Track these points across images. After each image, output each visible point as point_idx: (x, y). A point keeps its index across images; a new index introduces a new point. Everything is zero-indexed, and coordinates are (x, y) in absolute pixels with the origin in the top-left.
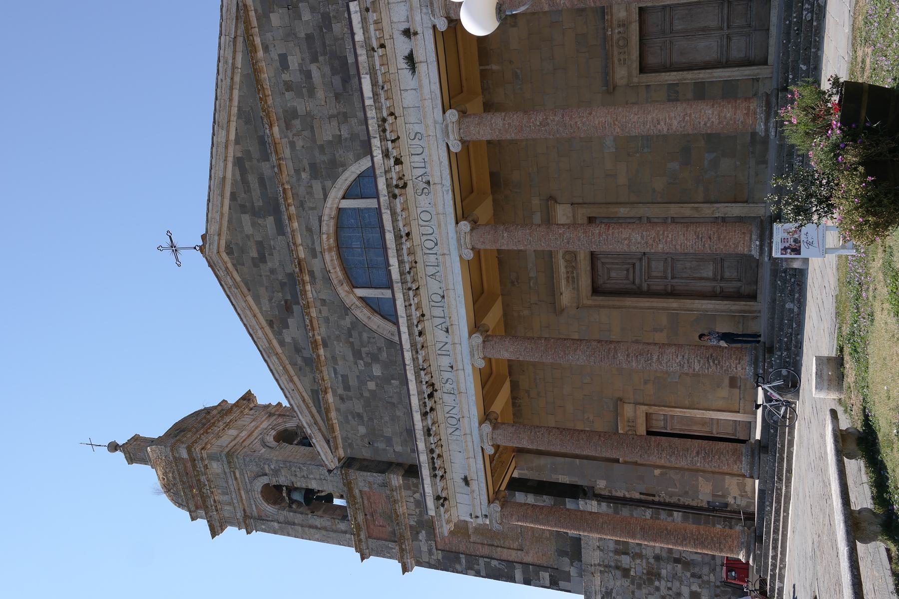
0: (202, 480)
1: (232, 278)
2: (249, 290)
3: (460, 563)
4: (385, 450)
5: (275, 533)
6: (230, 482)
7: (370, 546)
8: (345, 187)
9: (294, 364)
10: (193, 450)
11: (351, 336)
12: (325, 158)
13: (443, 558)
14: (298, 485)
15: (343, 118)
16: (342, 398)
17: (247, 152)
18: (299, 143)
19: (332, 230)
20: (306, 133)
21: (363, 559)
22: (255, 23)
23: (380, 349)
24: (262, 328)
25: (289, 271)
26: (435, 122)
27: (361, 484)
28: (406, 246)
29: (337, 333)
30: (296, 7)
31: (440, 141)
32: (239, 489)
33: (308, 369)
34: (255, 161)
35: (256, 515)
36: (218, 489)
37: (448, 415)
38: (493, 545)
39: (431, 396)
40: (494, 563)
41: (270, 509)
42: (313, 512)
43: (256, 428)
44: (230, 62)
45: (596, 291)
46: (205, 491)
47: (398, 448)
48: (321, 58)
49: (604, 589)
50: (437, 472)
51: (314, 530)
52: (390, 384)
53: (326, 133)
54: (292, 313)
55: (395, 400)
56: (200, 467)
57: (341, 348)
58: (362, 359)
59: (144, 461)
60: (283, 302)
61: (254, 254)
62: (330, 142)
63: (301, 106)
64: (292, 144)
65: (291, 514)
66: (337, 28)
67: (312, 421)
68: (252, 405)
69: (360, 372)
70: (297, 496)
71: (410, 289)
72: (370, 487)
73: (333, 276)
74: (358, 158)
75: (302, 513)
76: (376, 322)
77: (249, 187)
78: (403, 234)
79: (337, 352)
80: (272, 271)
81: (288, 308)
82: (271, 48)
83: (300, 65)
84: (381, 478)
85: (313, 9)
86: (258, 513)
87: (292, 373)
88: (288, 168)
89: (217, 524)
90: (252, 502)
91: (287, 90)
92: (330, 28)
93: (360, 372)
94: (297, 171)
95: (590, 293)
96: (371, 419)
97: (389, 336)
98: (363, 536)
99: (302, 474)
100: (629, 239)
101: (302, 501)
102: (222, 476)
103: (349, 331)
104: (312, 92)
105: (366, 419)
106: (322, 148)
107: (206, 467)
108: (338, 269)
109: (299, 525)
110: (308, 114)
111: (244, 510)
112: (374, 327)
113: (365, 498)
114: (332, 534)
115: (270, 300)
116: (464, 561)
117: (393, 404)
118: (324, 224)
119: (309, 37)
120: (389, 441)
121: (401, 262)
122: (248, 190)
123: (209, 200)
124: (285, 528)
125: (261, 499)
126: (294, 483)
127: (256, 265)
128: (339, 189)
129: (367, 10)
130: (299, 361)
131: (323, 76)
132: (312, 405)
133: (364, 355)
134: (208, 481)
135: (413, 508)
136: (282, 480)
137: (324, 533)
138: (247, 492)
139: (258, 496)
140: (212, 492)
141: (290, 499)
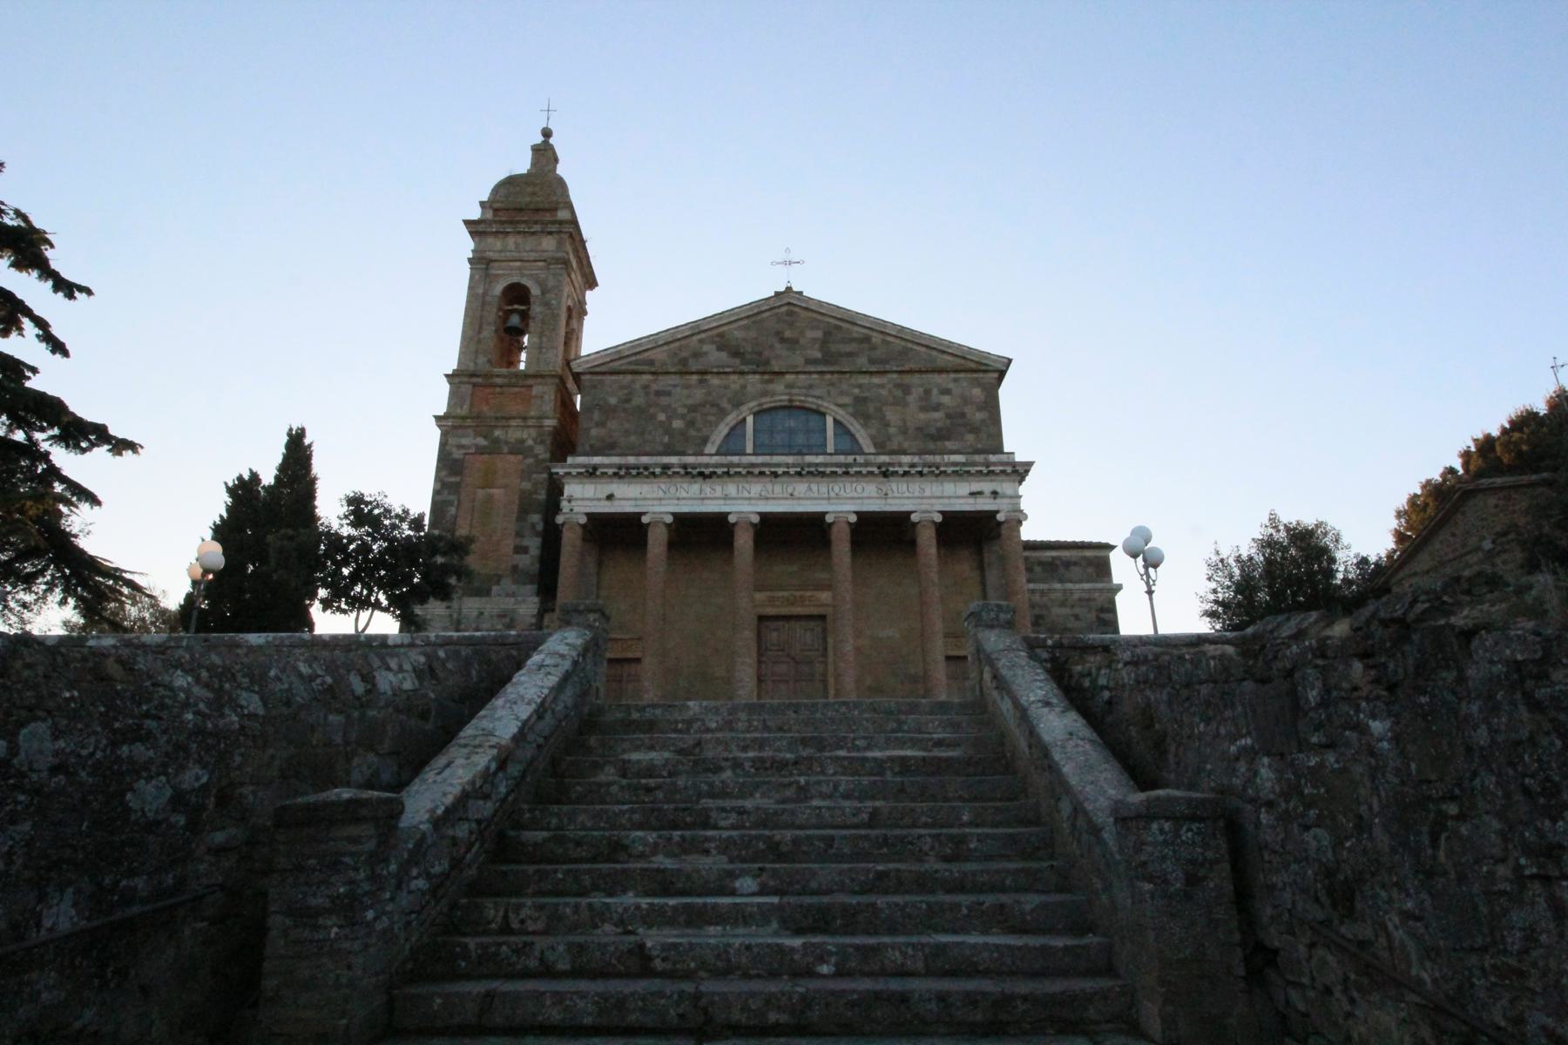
1: (766, 311)
5: (470, 288)
7: (462, 386)
8: (845, 422)
9: (680, 349)
11: (712, 405)
12: (871, 410)
13: (456, 460)
15: (904, 431)
19: (807, 405)
20: (891, 399)
21: (447, 376)
22: (975, 375)
23: (699, 430)
25: (773, 362)
26: (932, 505)
27: (540, 387)
28: (840, 471)
29: (714, 394)
38: (473, 511)
39: (701, 474)
40: (453, 510)
41: (498, 289)
45: (762, 618)
47: (594, 432)
48: (948, 422)
49: (429, 617)
53: (892, 415)
55: (648, 437)
57: (699, 394)
58: (689, 412)
60: (742, 351)
61: (788, 334)
62: (883, 418)
63: (911, 398)
64: (882, 386)
65: (495, 310)
66: (970, 438)
70: (515, 320)
71: (802, 469)
72: (535, 397)
73: (768, 399)
74: (873, 438)
76: (723, 429)
78: (850, 470)
80: (772, 347)
81: (736, 353)
85: (983, 421)
87: (672, 346)
89: (481, 228)
90: (509, 272)
92: (971, 431)
93: (675, 410)
94: (860, 386)
96: (625, 410)
97: (712, 438)
101: (509, 325)
103: (718, 405)
104: (924, 409)
105: (627, 406)
106: (879, 410)
107: (550, 233)
108: (773, 405)
110: (906, 405)
115: (745, 340)
116: (453, 479)
117: (642, 434)
118: (815, 400)
119: (963, 415)
120: (601, 424)
121: (826, 465)
127: (778, 333)
129: (1014, 467)
130: (684, 354)
131: (936, 420)
133: (693, 415)
136: (536, 309)
138: (519, 269)
139: (515, 280)
140: (519, 233)
141: (512, 311)
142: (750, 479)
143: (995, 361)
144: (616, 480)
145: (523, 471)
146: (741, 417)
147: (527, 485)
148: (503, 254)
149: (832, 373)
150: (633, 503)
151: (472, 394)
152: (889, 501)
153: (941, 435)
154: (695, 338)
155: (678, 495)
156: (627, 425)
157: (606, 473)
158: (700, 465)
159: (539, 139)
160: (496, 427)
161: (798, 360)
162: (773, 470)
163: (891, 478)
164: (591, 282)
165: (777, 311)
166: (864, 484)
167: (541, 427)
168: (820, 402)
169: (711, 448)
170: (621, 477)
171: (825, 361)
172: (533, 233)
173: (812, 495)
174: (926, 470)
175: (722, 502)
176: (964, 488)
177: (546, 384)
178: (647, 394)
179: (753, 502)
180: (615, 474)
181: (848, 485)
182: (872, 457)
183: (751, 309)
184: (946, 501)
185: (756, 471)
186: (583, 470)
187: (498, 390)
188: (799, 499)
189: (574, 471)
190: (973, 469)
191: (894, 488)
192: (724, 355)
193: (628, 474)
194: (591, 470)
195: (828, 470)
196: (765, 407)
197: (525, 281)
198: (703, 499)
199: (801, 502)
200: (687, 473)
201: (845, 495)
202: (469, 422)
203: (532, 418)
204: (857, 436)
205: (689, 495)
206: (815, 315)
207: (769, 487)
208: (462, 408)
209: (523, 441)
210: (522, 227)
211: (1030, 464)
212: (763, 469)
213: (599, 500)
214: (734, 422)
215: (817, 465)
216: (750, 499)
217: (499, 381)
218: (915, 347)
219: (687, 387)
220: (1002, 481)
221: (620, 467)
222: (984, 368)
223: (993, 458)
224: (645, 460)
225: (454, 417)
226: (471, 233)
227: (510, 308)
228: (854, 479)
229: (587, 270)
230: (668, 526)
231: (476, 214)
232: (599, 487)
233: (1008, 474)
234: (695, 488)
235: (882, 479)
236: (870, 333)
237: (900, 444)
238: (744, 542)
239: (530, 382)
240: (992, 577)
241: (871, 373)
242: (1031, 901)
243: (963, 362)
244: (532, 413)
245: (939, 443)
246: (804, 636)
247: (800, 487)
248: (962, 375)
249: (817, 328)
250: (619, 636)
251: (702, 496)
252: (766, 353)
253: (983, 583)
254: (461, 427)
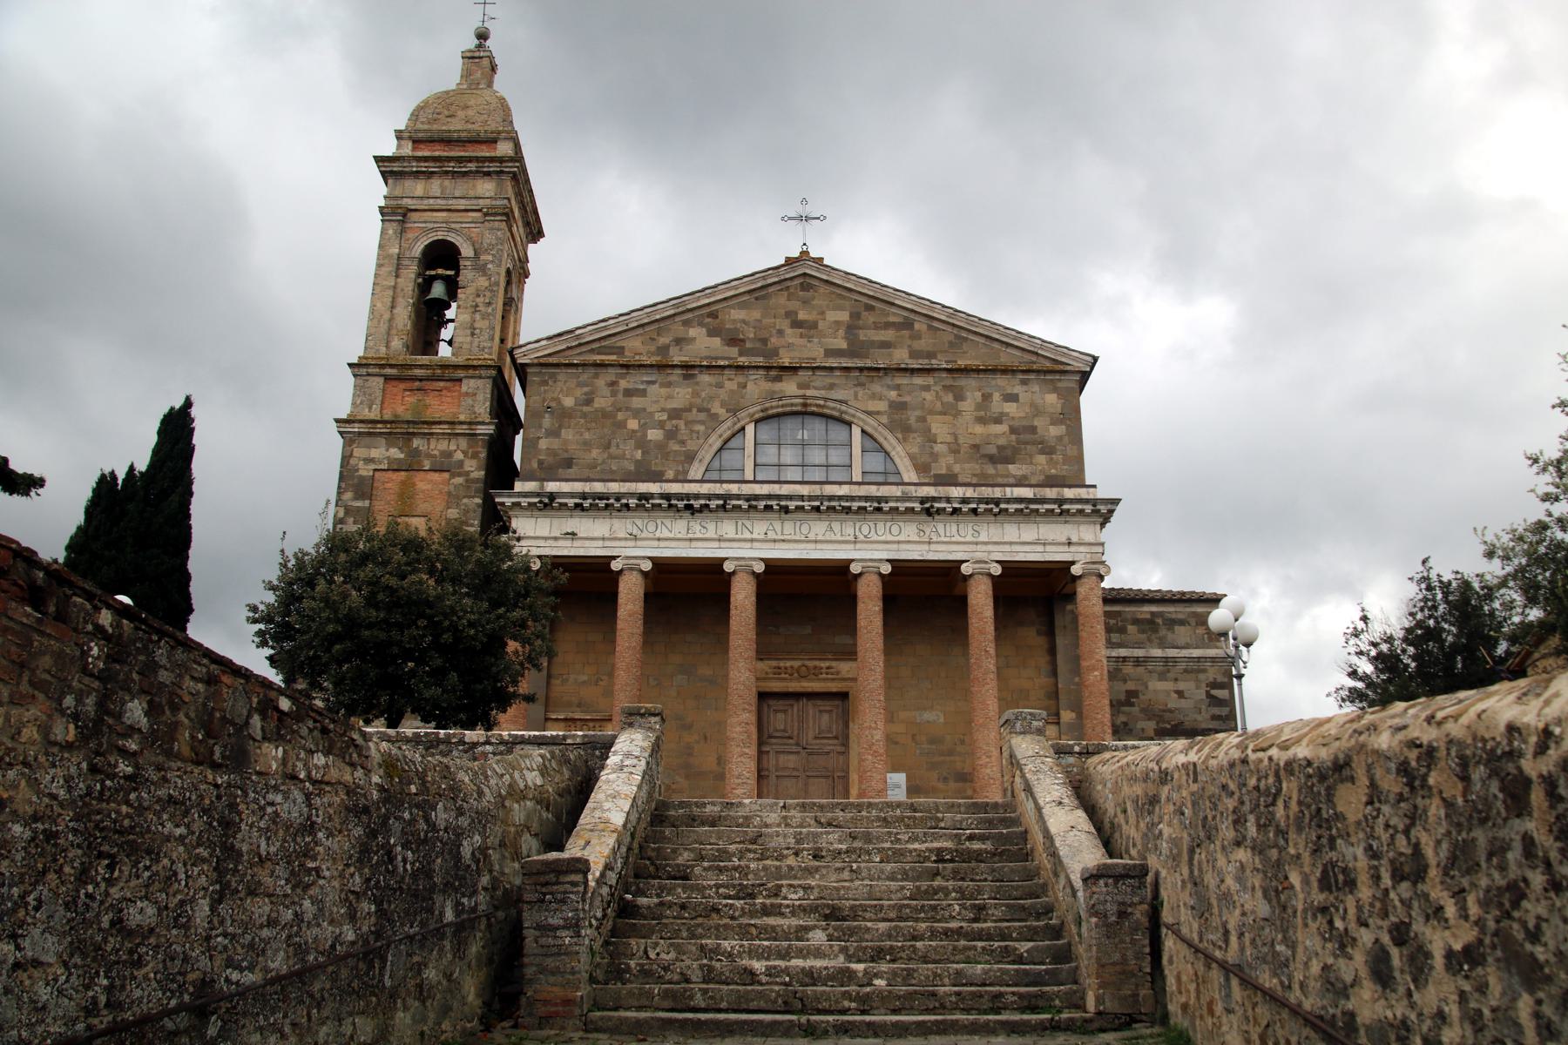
2: (757, 299)
3: (356, 498)
4: (540, 427)
5: (381, 246)
6: (463, 202)
8: (876, 435)
11: (700, 410)
12: (912, 421)
13: (361, 477)
14: (461, 294)
16: (613, 384)
17: (917, 336)
18: (929, 396)
20: (939, 404)
22: (1049, 377)
23: (683, 443)
24: (709, 304)
25: (781, 352)
26: (989, 552)
27: (472, 382)
29: (703, 395)
30: (1061, 422)
31: (971, 555)
33: (653, 348)
34: (909, 342)
37: (659, 522)
39: (689, 507)
44: (1016, 343)
50: (589, 501)
52: (637, 448)
53: (939, 427)
54: (728, 345)
55: (613, 450)
58: (670, 418)
59: (466, 74)
61: (802, 316)
63: (967, 406)
65: (413, 276)
69: (651, 414)
72: (467, 394)
77: (881, 328)
78: (883, 505)
79: (677, 390)
80: (781, 332)
81: (733, 340)
82: (1025, 388)
83: (1007, 415)
84: (482, 410)
85: (1060, 438)
87: (647, 329)
88: (903, 380)
89: (396, 167)
91: (983, 395)
92: (1042, 452)
93: (651, 414)
95: (761, 690)
96: (584, 415)
97: (699, 456)
98: (388, 371)
100: (876, 728)
102: (472, 193)
103: (708, 410)
104: (981, 420)
105: (585, 409)
106: (922, 419)
107: (488, 174)
108: (780, 410)
110: (958, 414)
112: (711, 441)
113: (448, 384)
114: (384, 327)
115: (744, 321)
116: (359, 504)
117: (608, 446)
119: (1033, 429)
120: (554, 433)
122: (877, 326)
123: (871, 281)
124: (389, 263)
127: (788, 314)
128: (876, 430)
129: (1094, 505)
130: (664, 340)
131: (996, 436)
135: (439, 447)
136: (466, 275)
137: (387, 316)
139: (440, 236)
142: (752, 514)
143: (1075, 359)
144: (578, 512)
145: (449, 494)
146: (738, 426)
147: (453, 513)
148: (426, 202)
149: (861, 369)
150: (600, 543)
151: (384, 390)
152: (933, 547)
153: (1004, 456)
154: (678, 319)
155: (658, 534)
156: (587, 436)
157: (566, 504)
158: (688, 496)
159: (472, 42)
160: (414, 434)
161: (813, 351)
162: (783, 503)
163: (937, 517)
164: (536, 233)
165: (789, 283)
166: (901, 524)
167: (475, 435)
168: (844, 408)
169: (696, 471)
170: (583, 509)
171: (851, 353)
172: (465, 174)
173: (833, 538)
174: (983, 507)
175: (716, 544)
176: (1029, 532)
177: (480, 377)
178: (614, 394)
179: (756, 545)
180: (577, 506)
181: (880, 525)
182: (912, 488)
183: (752, 282)
184: (1007, 548)
185: (762, 504)
186: (536, 500)
187: (417, 384)
188: (816, 542)
189: (524, 502)
190: (1043, 508)
191: (941, 531)
192: (717, 341)
193: (594, 507)
194: (546, 501)
195: (855, 505)
196: (771, 412)
197: (452, 238)
198: (691, 540)
199: (819, 546)
200: (670, 506)
201: (875, 538)
202: (380, 428)
203: (461, 423)
204: (893, 454)
205: (671, 535)
206: (839, 291)
207: (778, 527)
208: (370, 408)
209: (449, 454)
210: (451, 166)
211: (1116, 502)
212: (769, 503)
213: (556, 539)
214: (729, 433)
215: (840, 498)
216: (752, 540)
217: (418, 372)
218: (971, 337)
219: (669, 385)
220: (1079, 523)
221: (584, 496)
222: (1061, 367)
223: (1069, 493)
224: (614, 487)
225: (362, 421)
226: (383, 174)
227: (433, 273)
228: (889, 517)
229: (531, 219)
230: (645, 574)
231: (389, 148)
232: (556, 521)
233: (1088, 515)
234: (678, 526)
235: (924, 517)
236: (912, 316)
237: (949, 468)
238: (743, 596)
239: (461, 374)
240: (1061, 642)
241: (913, 371)
242: (1024, 946)
243: (1034, 358)
244: (462, 418)
245: (999, 466)
246: (819, 719)
247: (818, 528)
248: (1032, 376)
249: (841, 308)
250: (577, 716)
251: (690, 536)
252: (774, 341)
253: (1052, 651)
254: (370, 434)
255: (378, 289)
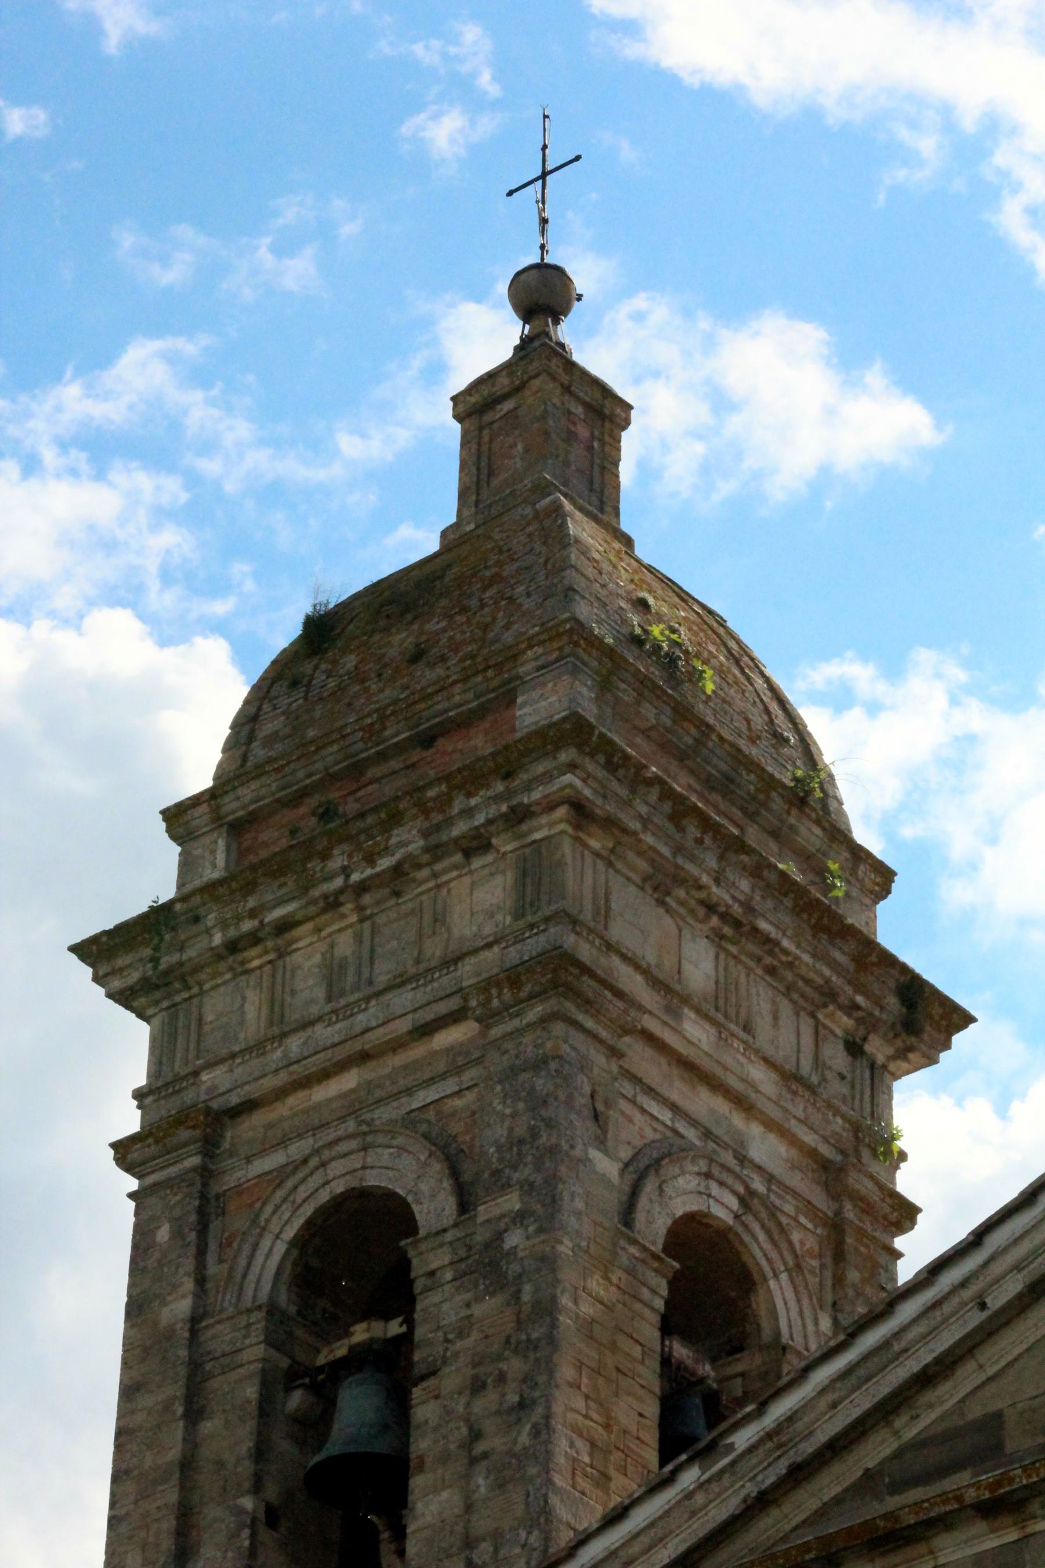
0: (398, 835)
6: (404, 999)
10: (565, 756)
32: (364, 1057)
35: (230, 1180)
36: (358, 939)
42: (272, 1516)
43: (742, 1103)
46: (337, 861)
51: (167, 1543)
56: (468, 812)
65: (251, 1392)
67: (808, 1448)
68: (877, 1048)
75: (261, 1453)
86: (239, 1190)
90: (297, 1149)
99: (489, 1426)
101: (333, 1448)
102: (434, 949)
109: (191, 1442)
111: (249, 1106)
125: (324, 1196)
126: (431, 1382)
132: (910, 1434)
134: (397, 870)
140: (332, 903)
141: (340, 1369)
255: (130, 1486)
